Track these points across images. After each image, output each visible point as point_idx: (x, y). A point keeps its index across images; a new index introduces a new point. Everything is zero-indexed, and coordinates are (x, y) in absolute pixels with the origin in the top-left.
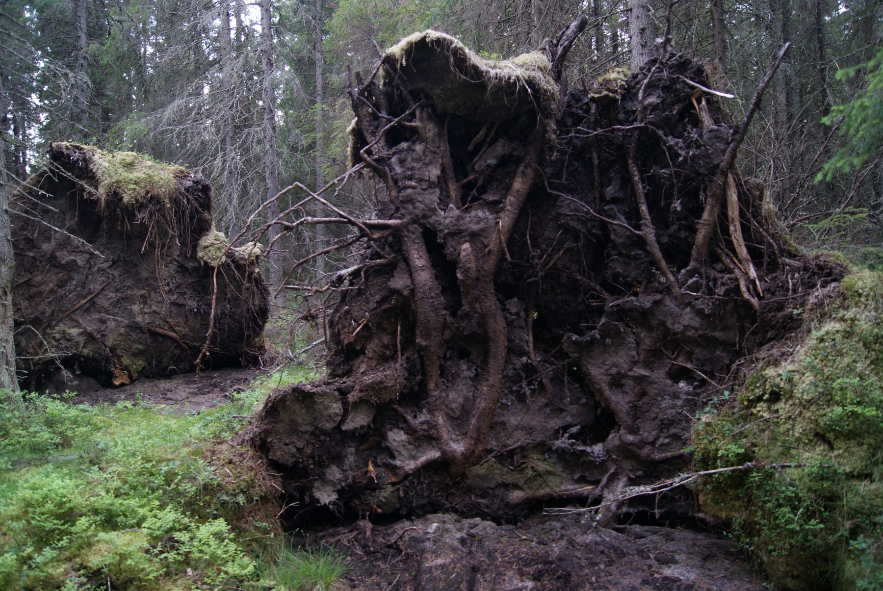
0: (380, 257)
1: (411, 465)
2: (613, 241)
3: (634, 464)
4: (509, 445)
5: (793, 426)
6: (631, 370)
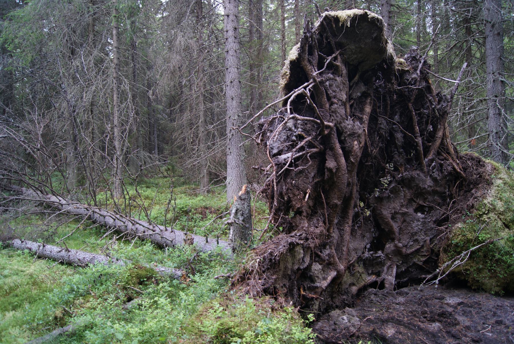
0: (314, 147)
1: (324, 284)
2: (396, 143)
3: (399, 258)
4: (351, 261)
5: (497, 223)
6: (400, 210)
